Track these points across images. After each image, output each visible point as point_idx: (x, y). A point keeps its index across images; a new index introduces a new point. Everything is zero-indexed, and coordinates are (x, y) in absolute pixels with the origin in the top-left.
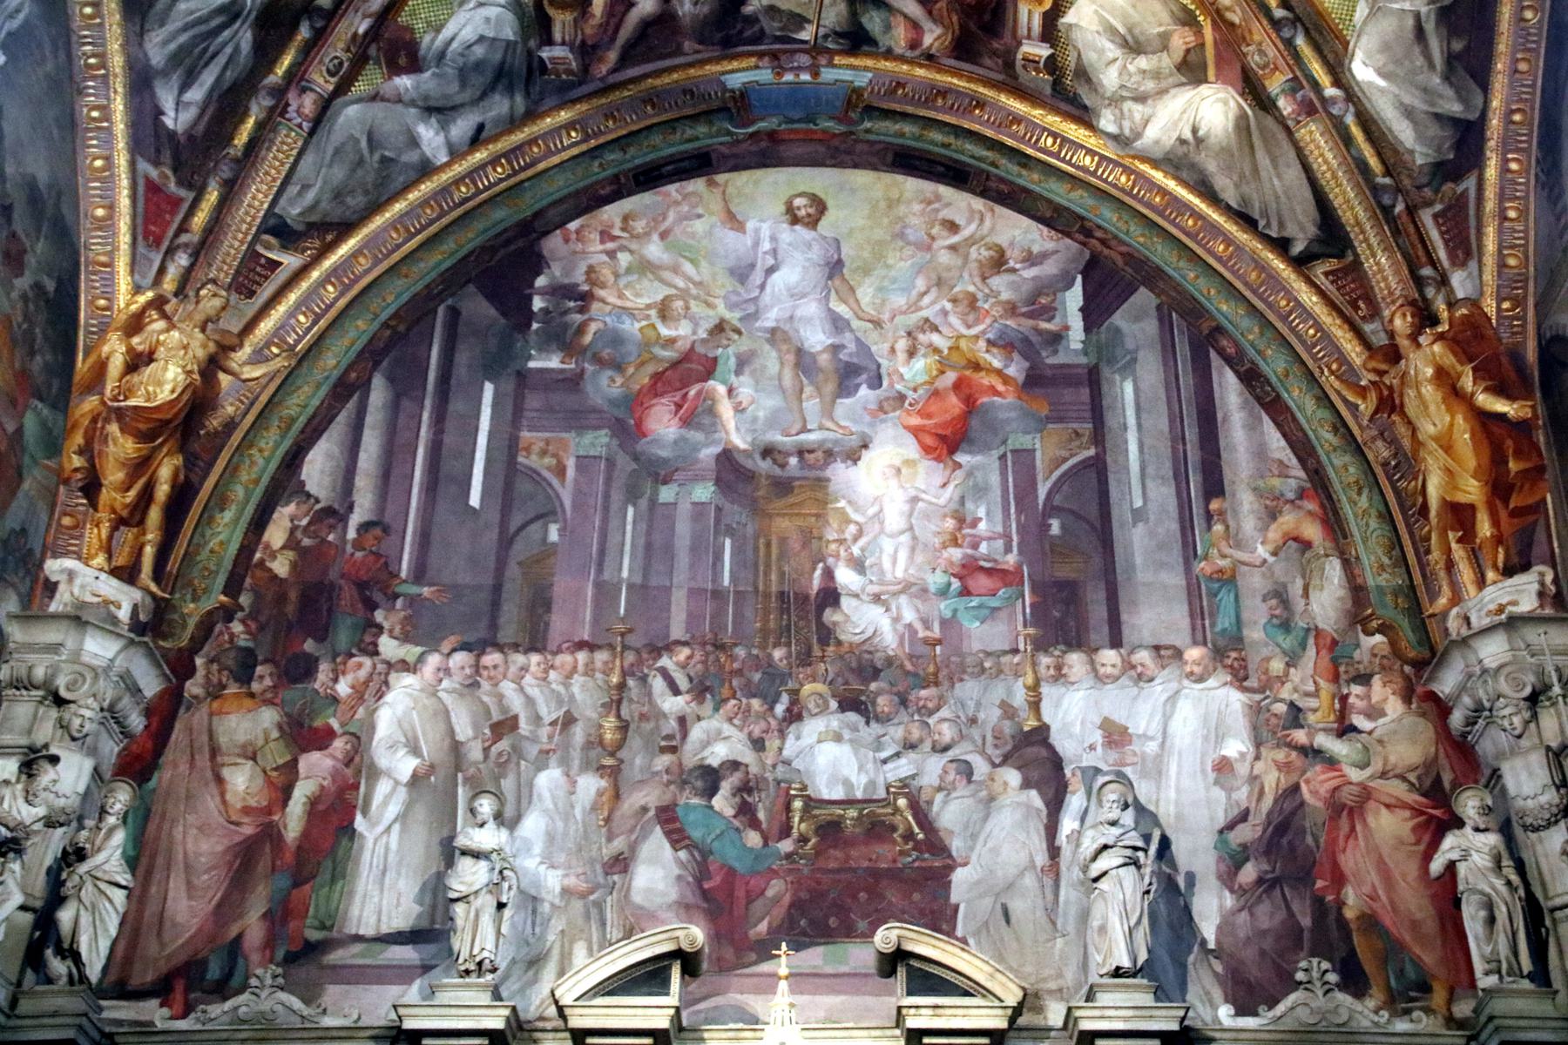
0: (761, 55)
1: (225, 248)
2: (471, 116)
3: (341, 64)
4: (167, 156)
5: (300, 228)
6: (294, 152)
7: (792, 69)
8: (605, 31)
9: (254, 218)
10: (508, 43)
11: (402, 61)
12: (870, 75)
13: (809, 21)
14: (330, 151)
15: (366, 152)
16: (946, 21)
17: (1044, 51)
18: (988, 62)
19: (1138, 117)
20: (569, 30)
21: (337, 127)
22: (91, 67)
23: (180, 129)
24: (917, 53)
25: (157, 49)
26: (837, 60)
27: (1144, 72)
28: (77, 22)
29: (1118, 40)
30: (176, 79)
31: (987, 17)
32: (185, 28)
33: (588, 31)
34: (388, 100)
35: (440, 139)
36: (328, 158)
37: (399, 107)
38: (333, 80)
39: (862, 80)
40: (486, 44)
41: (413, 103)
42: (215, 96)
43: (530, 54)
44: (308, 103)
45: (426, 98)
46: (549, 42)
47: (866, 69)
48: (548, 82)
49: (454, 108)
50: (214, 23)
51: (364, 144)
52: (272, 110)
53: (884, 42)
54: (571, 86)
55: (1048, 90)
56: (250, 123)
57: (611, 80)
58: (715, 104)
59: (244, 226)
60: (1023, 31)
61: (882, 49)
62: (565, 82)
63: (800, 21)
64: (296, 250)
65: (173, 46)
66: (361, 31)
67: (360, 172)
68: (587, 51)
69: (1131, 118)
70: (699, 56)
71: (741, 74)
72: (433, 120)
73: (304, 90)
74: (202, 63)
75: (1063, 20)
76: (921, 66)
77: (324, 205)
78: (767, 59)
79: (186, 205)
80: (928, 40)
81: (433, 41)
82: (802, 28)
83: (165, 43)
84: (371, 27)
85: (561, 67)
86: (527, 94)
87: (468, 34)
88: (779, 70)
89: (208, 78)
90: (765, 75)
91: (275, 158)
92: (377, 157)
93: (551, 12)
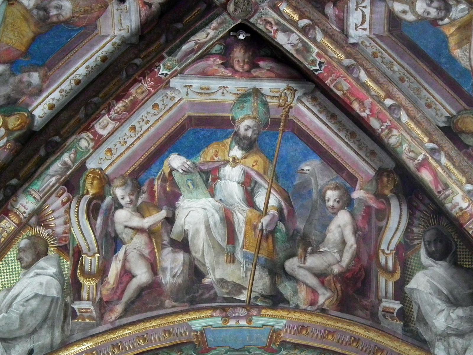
0: (215, 309)
2: (25, 345)
7: (235, 317)
8: (115, 292)
10: (53, 299)
12: (285, 322)
13: (245, 289)
16: (333, 287)
17: (396, 306)
18: (360, 312)
19: (459, 346)
24: (314, 308)
26: (263, 312)
27: (461, 318)
29: (443, 298)
31: (359, 285)
33: (104, 292)
39: (279, 324)
40: (38, 299)
43: (66, 305)
46: (79, 298)
47: (282, 317)
48: (77, 324)
53: (293, 301)
54: (92, 326)
55: (400, 331)
57: (117, 323)
58: (184, 339)
60: (382, 293)
61: (292, 306)
63: (240, 288)
68: (103, 306)
69: (455, 348)
70: (175, 310)
71: (200, 321)
75: (408, 286)
76: (317, 316)
78: (218, 311)
80: (321, 300)
82: (241, 293)
85: (86, 315)
86: (63, 330)
87: (28, 292)
88: (226, 319)
90: (217, 321)
93: (81, 280)
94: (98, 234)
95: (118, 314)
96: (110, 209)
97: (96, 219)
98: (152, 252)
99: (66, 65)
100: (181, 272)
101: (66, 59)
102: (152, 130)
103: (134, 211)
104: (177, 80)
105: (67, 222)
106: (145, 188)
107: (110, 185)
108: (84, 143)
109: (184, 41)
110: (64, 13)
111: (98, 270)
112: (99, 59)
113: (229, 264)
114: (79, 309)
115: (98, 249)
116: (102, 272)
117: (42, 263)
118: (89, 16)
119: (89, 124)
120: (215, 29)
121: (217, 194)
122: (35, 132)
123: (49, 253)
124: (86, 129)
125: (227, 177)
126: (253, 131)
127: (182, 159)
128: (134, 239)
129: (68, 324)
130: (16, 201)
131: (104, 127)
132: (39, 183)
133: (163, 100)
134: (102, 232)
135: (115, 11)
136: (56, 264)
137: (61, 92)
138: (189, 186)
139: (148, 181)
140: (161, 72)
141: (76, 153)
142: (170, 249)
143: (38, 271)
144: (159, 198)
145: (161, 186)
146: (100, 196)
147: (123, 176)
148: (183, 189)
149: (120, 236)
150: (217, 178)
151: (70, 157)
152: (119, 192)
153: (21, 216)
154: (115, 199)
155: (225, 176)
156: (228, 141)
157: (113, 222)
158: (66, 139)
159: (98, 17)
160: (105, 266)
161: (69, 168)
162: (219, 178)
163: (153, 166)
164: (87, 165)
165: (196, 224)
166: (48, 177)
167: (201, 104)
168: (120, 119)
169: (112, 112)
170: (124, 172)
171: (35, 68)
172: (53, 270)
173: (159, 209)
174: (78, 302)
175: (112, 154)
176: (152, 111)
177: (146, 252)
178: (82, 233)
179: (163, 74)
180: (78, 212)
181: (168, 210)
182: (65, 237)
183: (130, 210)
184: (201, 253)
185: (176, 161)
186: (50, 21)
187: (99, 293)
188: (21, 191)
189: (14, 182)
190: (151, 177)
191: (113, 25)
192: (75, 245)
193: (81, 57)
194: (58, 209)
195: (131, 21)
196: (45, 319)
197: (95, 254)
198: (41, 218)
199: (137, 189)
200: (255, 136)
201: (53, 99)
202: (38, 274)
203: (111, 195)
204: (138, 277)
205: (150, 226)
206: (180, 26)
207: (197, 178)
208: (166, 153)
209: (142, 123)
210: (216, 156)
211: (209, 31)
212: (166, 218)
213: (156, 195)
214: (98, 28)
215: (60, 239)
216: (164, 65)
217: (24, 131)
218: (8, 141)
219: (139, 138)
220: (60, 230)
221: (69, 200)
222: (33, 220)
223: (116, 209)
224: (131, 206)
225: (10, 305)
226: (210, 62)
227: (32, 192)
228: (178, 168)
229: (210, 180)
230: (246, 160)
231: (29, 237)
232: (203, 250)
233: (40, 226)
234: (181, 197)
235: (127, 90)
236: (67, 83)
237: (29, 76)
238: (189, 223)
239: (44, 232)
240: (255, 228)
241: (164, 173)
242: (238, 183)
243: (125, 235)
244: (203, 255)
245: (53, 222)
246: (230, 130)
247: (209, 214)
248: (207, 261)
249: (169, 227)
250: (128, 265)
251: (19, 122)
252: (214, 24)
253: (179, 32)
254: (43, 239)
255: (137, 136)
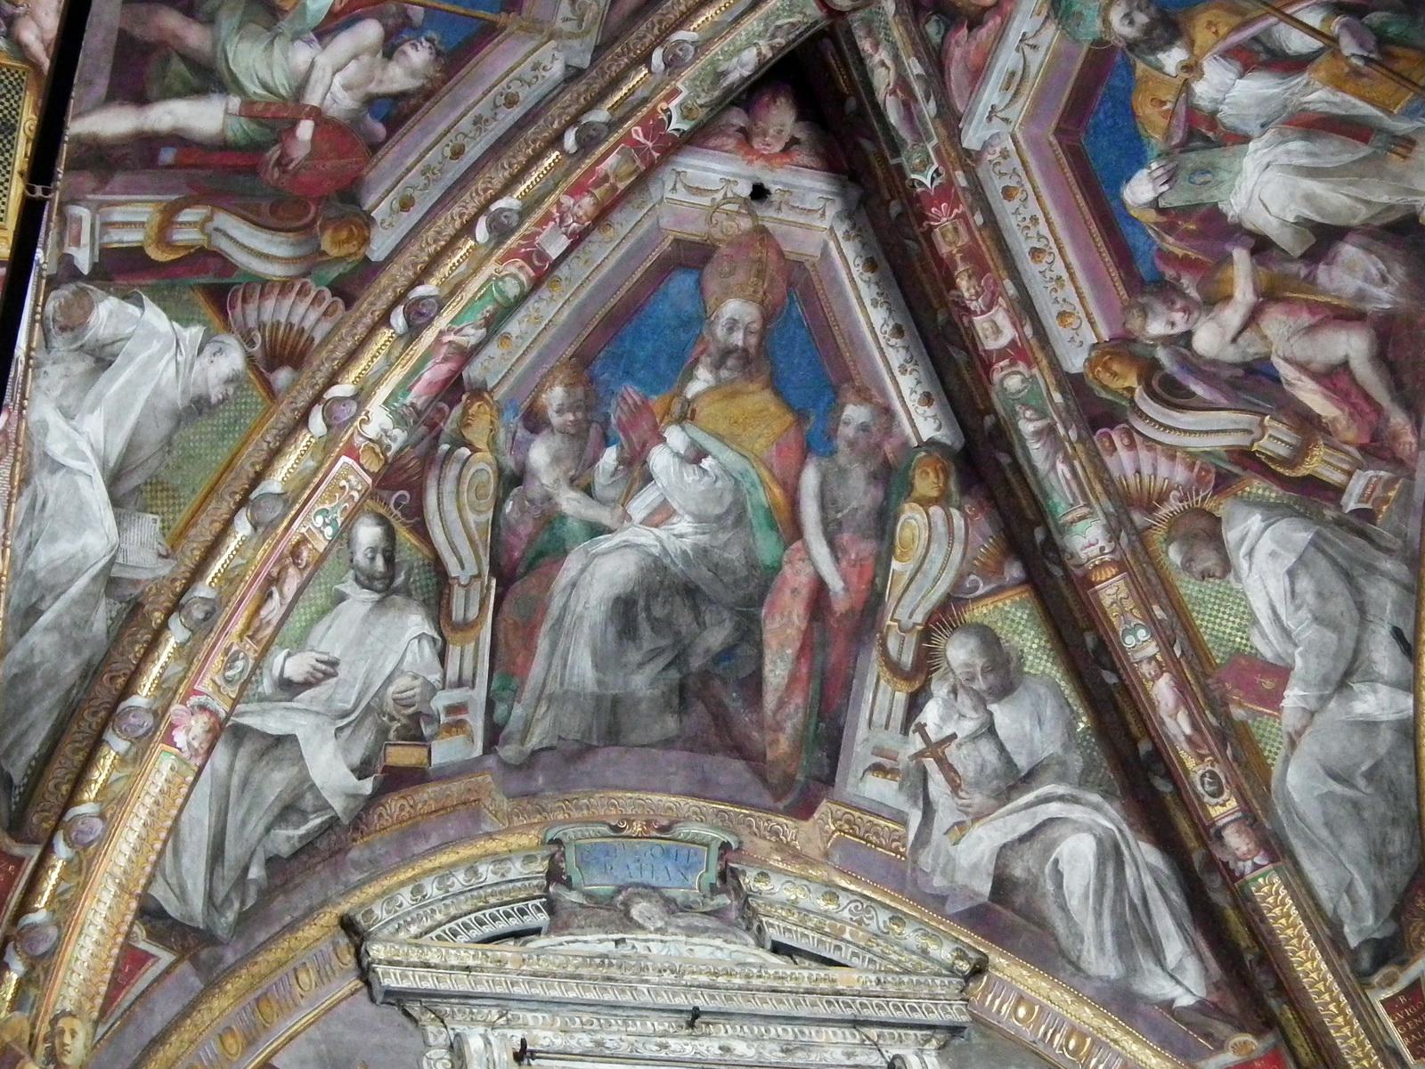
1: (1343, 1047)
2: (1379, 638)
3: (1213, 775)
4: (1220, 1028)
5: (1391, 928)
6: (1283, 892)
8: (1361, 413)
9: (1329, 990)
10: (1313, 543)
11: (1268, 684)
14: (1324, 833)
15: (1349, 792)
20: (1337, 458)
21: (1302, 808)
22: (1075, 1053)
23: (1201, 992)
25: (1102, 963)
28: (1027, 1034)
30: (1147, 964)
32: (1098, 915)
33: (1350, 435)
34: (1305, 728)
35: (1384, 691)
36: (1330, 840)
37: (1318, 719)
38: (1225, 796)
40: (1301, 572)
41: (1323, 700)
42: (1188, 925)
43: (1339, 523)
44: (1237, 842)
45: (1325, 680)
46: (1339, 491)
49: (1356, 652)
50: (1110, 881)
51: (1337, 788)
52: (1225, 883)
56: (1231, 914)
59: (1332, 1007)
62: (1396, 500)
64: (1413, 953)
65: (1109, 942)
66: (1188, 731)
67: (1367, 814)
68: (1377, 449)
72: (1355, 686)
73: (1219, 836)
74: (1145, 920)
77: (1380, 884)
79: (1283, 1050)
81: (1264, 635)
83: (1101, 949)
84: (1191, 715)
85: (1378, 492)
86: (1388, 551)
87: (1278, 587)
89: (1165, 924)
91: (1276, 919)
92: (1361, 783)
93: (1302, 471)
94: (1224, 402)
95: (1408, 428)
96: (1185, 358)
97: (1194, 394)
98: (1313, 307)
99: (852, 343)
100: (1384, 262)
101: (839, 340)
102: (1054, 215)
103: (1210, 311)
104: (971, 133)
105: (1171, 453)
106: (1170, 273)
107: (1135, 341)
108: (1014, 383)
109: (881, 115)
110: (748, 319)
111: (1297, 431)
112: (868, 275)
113: (1412, 155)
114: (1360, 501)
115: (1256, 413)
116: (1307, 423)
117: (1231, 536)
118: (771, 268)
119: (980, 356)
120: (876, 46)
121: (1247, 128)
122: (964, 449)
123: (1218, 514)
124: (988, 367)
125: (1220, 96)
126: (1140, 9)
127: (1142, 174)
128: (1268, 332)
129: (1380, 535)
130: (1072, 556)
131: (997, 331)
132: (1056, 499)
133: (1001, 174)
134: (1220, 390)
135: (780, 216)
136: (1246, 510)
137: (903, 371)
138: (1205, 183)
139: (1157, 262)
140: (927, 182)
141: (1027, 406)
142: (1322, 267)
143: (1244, 550)
144: (1204, 252)
145: (1180, 238)
146: (1149, 370)
147: (1126, 309)
148: (1205, 197)
149: (1249, 359)
150: (1212, 119)
151: (1030, 420)
152: (1157, 328)
153: (1107, 558)
154: (1168, 341)
155: (1214, 100)
156: (1141, 67)
157: (1214, 362)
158: (991, 410)
159: (781, 253)
160: (1297, 414)
161: (1051, 429)
162: (1214, 113)
163: (1130, 241)
164: (1073, 371)
165: (1292, 195)
166: (1052, 475)
167: (1038, 101)
168: (993, 293)
169: (973, 306)
170: (1118, 303)
171: (836, 407)
172: (1256, 521)
173: (1227, 259)
174: (1345, 497)
175: (1071, 314)
176: (1016, 202)
177: (1306, 319)
178: (1207, 432)
179: (933, 179)
180: (1161, 425)
181: (1236, 243)
182: (1201, 469)
183: (1203, 319)
184: (1359, 206)
185: (1140, 190)
186: (752, 351)
187: (1347, 448)
188: (1057, 537)
189: (1039, 535)
190: (1153, 252)
191: (809, 227)
192: (1225, 455)
193: (848, 309)
194: (1137, 460)
195: (812, 190)
196: (1348, 577)
197: (1263, 428)
198: (1141, 500)
199: (1166, 291)
200: (1153, 9)
201: (913, 391)
202: (1250, 554)
203: (1154, 346)
204: (1352, 354)
205: (1255, 290)
206: (851, 103)
207: (1194, 159)
208: (1114, 204)
209: (1032, 233)
210: (1163, 103)
211: (877, 58)
212: (1254, 252)
213: (1192, 255)
214: (803, 259)
215: (1200, 479)
216: (914, 171)
217: (953, 468)
218: (960, 508)
219: (1060, 249)
220: (1181, 475)
221: (1130, 432)
222: (1138, 518)
223: (1189, 346)
224: (1196, 315)
225: (1286, 633)
226: (957, 53)
227: (1069, 518)
228: (1155, 189)
229: (1210, 134)
230: (1198, 43)
231: (1169, 540)
232: (1357, 199)
233: (1155, 509)
234: (1220, 206)
235: (939, 260)
236: (890, 353)
237: (847, 424)
238: (1283, 209)
239: (1173, 505)
240: (1356, 73)
241: (1156, 224)
242: (1241, 76)
243: (1250, 348)
244: (1368, 203)
245: (1160, 480)
246: (1118, 58)
247: (1284, 160)
248: (1385, 199)
249: (1275, 253)
250: (1314, 366)
251: (932, 475)
252: (866, 45)
253: (860, 113)
254: (1184, 512)
255: (1055, 250)
